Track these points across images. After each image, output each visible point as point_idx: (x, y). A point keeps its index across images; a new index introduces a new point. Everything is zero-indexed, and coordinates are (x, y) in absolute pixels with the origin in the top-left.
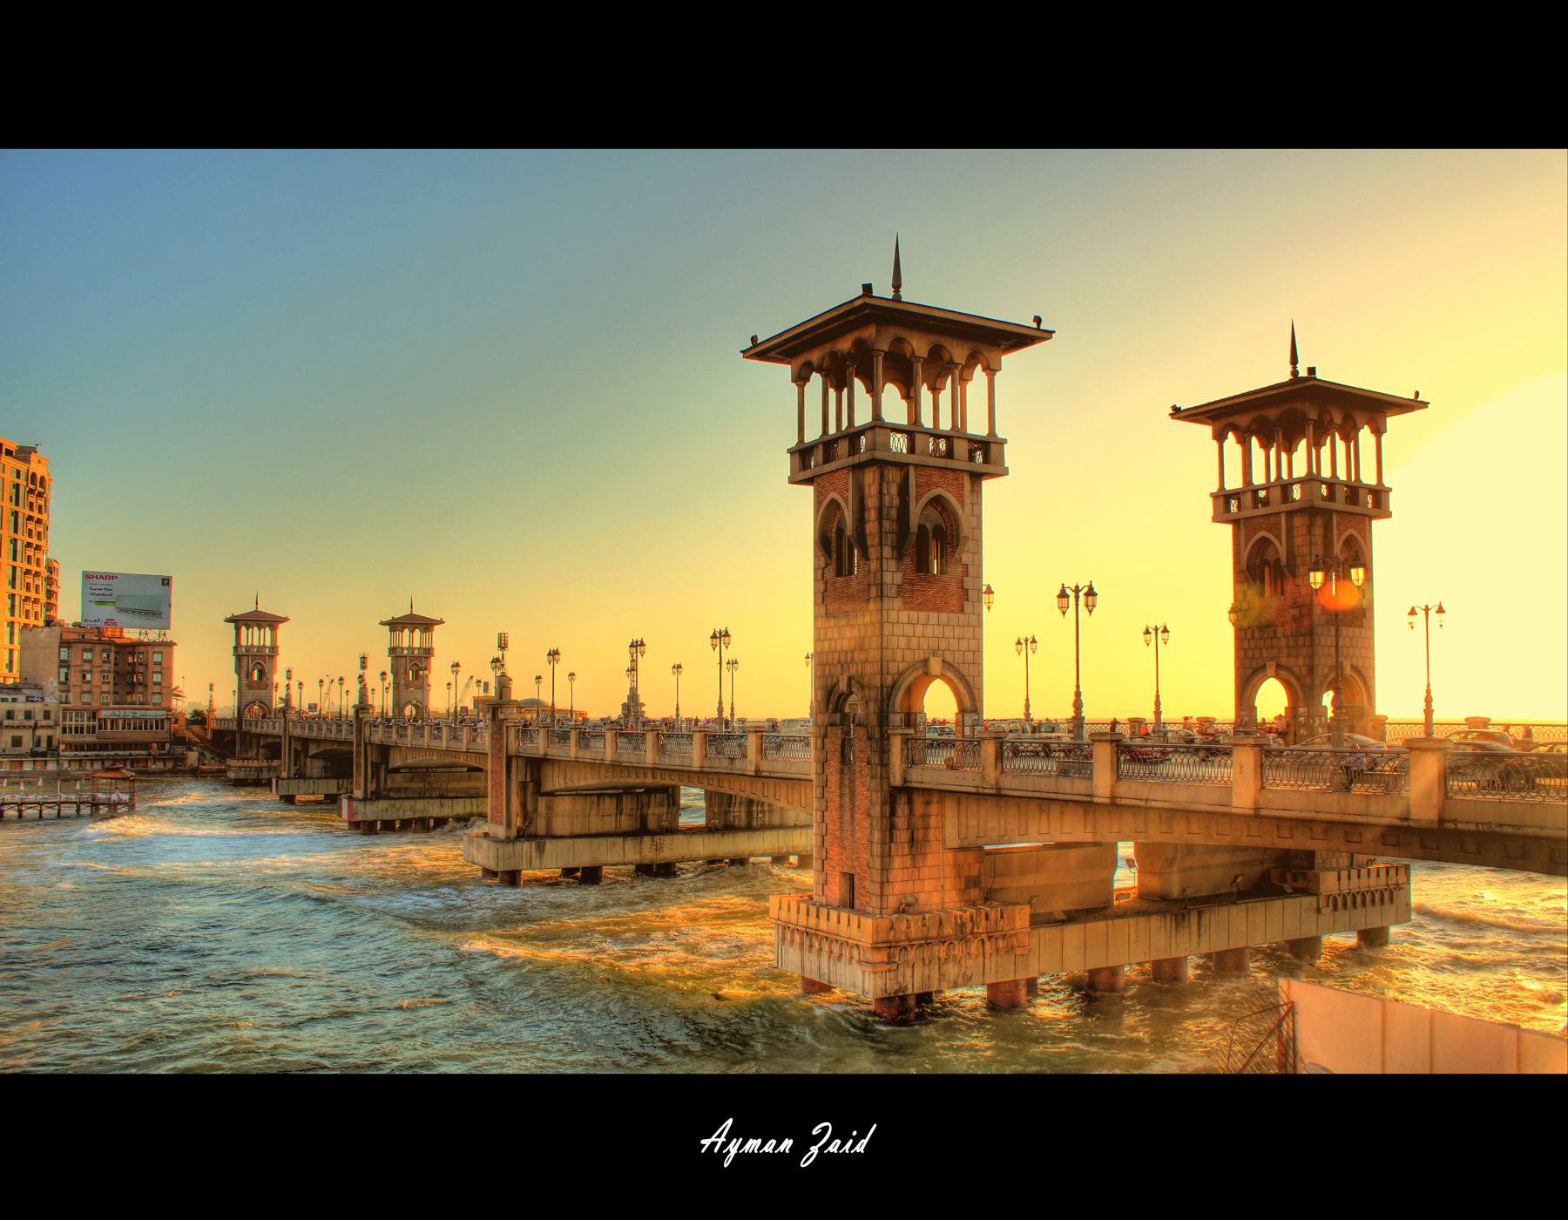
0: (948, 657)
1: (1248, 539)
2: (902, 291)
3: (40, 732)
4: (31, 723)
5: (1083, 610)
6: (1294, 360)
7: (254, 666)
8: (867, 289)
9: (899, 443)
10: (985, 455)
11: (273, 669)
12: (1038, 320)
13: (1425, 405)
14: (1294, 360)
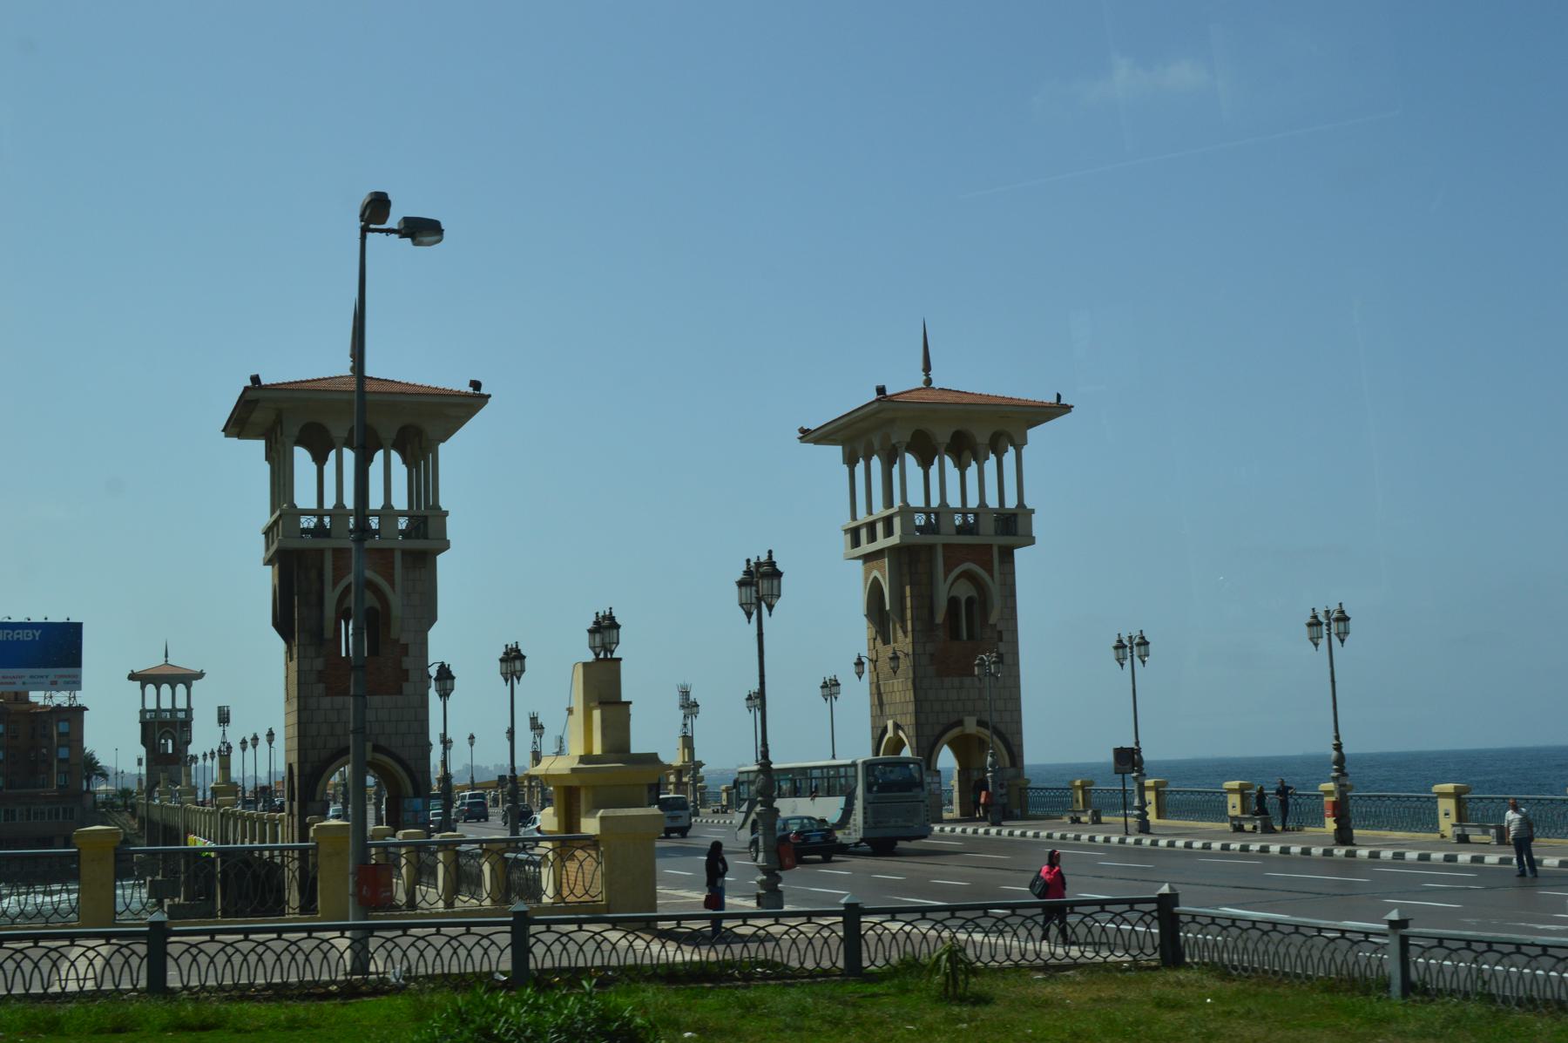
0: (382, 742)
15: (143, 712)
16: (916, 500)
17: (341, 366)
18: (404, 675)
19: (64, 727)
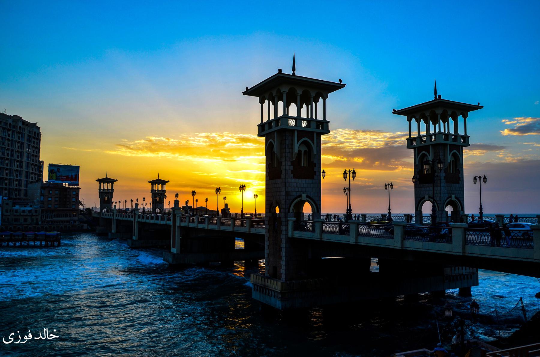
1: (418, 155)
2: (296, 72)
3: (33, 217)
4: (31, 214)
5: (351, 178)
6: (436, 93)
7: (106, 196)
8: (280, 71)
9: (291, 123)
10: (323, 127)
11: (112, 197)
12: (340, 81)
13: (482, 107)
14: (436, 93)
15: (100, 189)
16: (432, 132)
17: (291, 73)
18: (315, 173)
19: (74, 193)
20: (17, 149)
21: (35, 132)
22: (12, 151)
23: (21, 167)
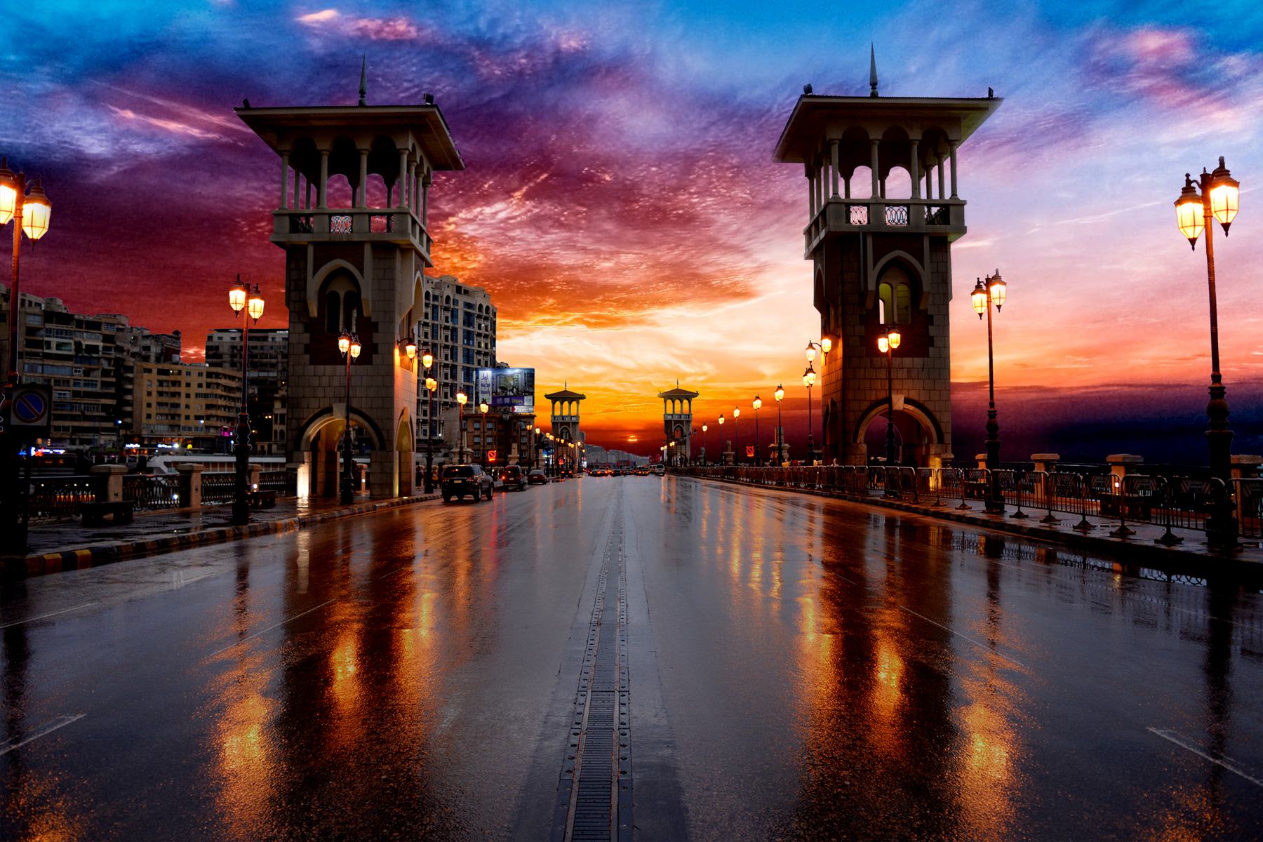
20: (444, 342)
21: (481, 306)
22: (434, 345)
23: (454, 376)
